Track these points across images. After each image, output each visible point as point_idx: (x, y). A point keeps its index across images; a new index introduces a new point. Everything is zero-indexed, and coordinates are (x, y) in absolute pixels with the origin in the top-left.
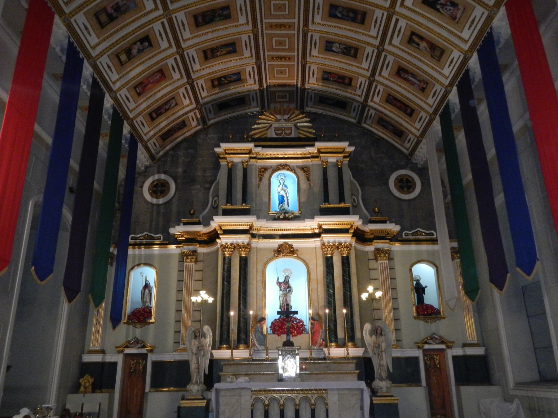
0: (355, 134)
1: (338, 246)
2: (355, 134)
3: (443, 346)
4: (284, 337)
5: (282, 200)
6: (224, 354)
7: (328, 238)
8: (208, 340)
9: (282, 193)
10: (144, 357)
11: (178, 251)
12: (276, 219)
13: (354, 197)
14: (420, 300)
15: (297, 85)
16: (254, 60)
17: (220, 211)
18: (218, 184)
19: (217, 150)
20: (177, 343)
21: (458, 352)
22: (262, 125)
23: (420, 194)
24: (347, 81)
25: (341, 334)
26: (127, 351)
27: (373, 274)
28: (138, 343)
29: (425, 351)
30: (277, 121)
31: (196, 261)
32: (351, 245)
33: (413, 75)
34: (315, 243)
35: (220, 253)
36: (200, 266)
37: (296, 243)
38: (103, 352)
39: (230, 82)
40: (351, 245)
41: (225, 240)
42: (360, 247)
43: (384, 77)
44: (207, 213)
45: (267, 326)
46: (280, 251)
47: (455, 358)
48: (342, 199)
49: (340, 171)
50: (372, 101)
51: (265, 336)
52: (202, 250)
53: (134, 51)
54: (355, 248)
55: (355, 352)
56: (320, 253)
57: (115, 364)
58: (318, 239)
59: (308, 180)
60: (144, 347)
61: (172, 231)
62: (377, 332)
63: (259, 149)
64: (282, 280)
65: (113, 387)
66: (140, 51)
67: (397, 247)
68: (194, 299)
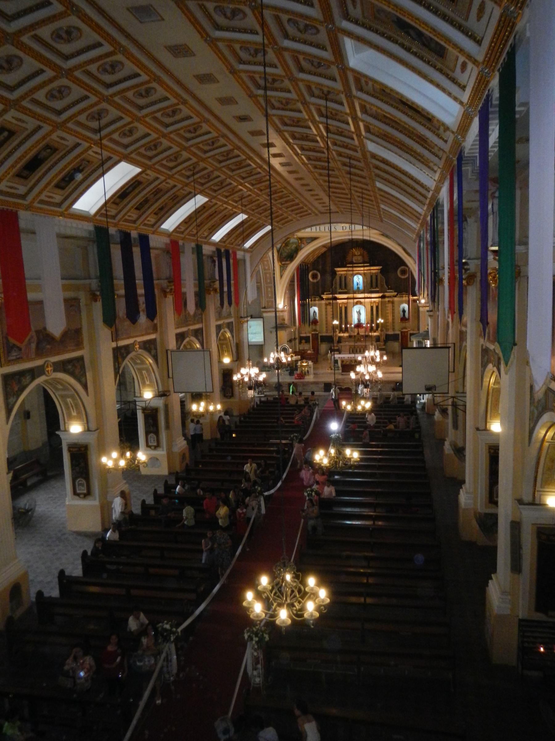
1: (374, 302)
3: (406, 330)
5: (358, 284)
6: (342, 335)
8: (338, 332)
10: (318, 334)
12: (354, 292)
19: (336, 269)
20: (327, 330)
28: (315, 330)
29: (402, 332)
37: (362, 300)
42: (384, 300)
46: (357, 303)
49: (377, 276)
61: (322, 296)
67: (396, 299)
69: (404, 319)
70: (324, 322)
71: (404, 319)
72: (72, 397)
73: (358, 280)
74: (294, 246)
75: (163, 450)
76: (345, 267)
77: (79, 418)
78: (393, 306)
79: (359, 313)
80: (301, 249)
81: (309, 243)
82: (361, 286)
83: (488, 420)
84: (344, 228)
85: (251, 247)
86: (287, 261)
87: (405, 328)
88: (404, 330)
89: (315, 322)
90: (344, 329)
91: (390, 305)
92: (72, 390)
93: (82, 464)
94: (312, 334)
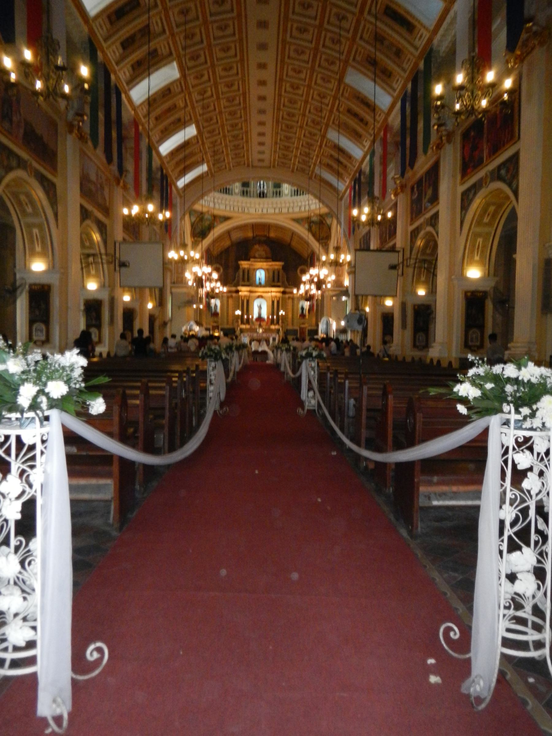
1: (276, 297)
4: (259, 323)
5: (259, 279)
6: (243, 326)
12: (257, 286)
18: (239, 274)
21: (310, 328)
25: (275, 322)
30: (258, 250)
45: (254, 319)
46: (259, 297)
48: (278, 281)
49: (279, 272)
52: (234, 295)
55: (277, 327)
59: (269, 273)
62: (283, 322)
64: (259, 305)
69: (303, 315)
70: (225, 314)
71: (303, 315)
72: (40, 227)
73: (261, 275)
75: (105, 346)
77: (44, 254)
78: (293, 302)
79: (260, 308)
80: (213, 228)
82: (263, 281)
83: (465, 266)
84: (257, 210)
85: (187, 186)
86: (199, 237)
87: (303, 324)
89: (215, 314)
90: (245, 321)
91: (290, 301)
92: (44, 217)
93: (43, 306)
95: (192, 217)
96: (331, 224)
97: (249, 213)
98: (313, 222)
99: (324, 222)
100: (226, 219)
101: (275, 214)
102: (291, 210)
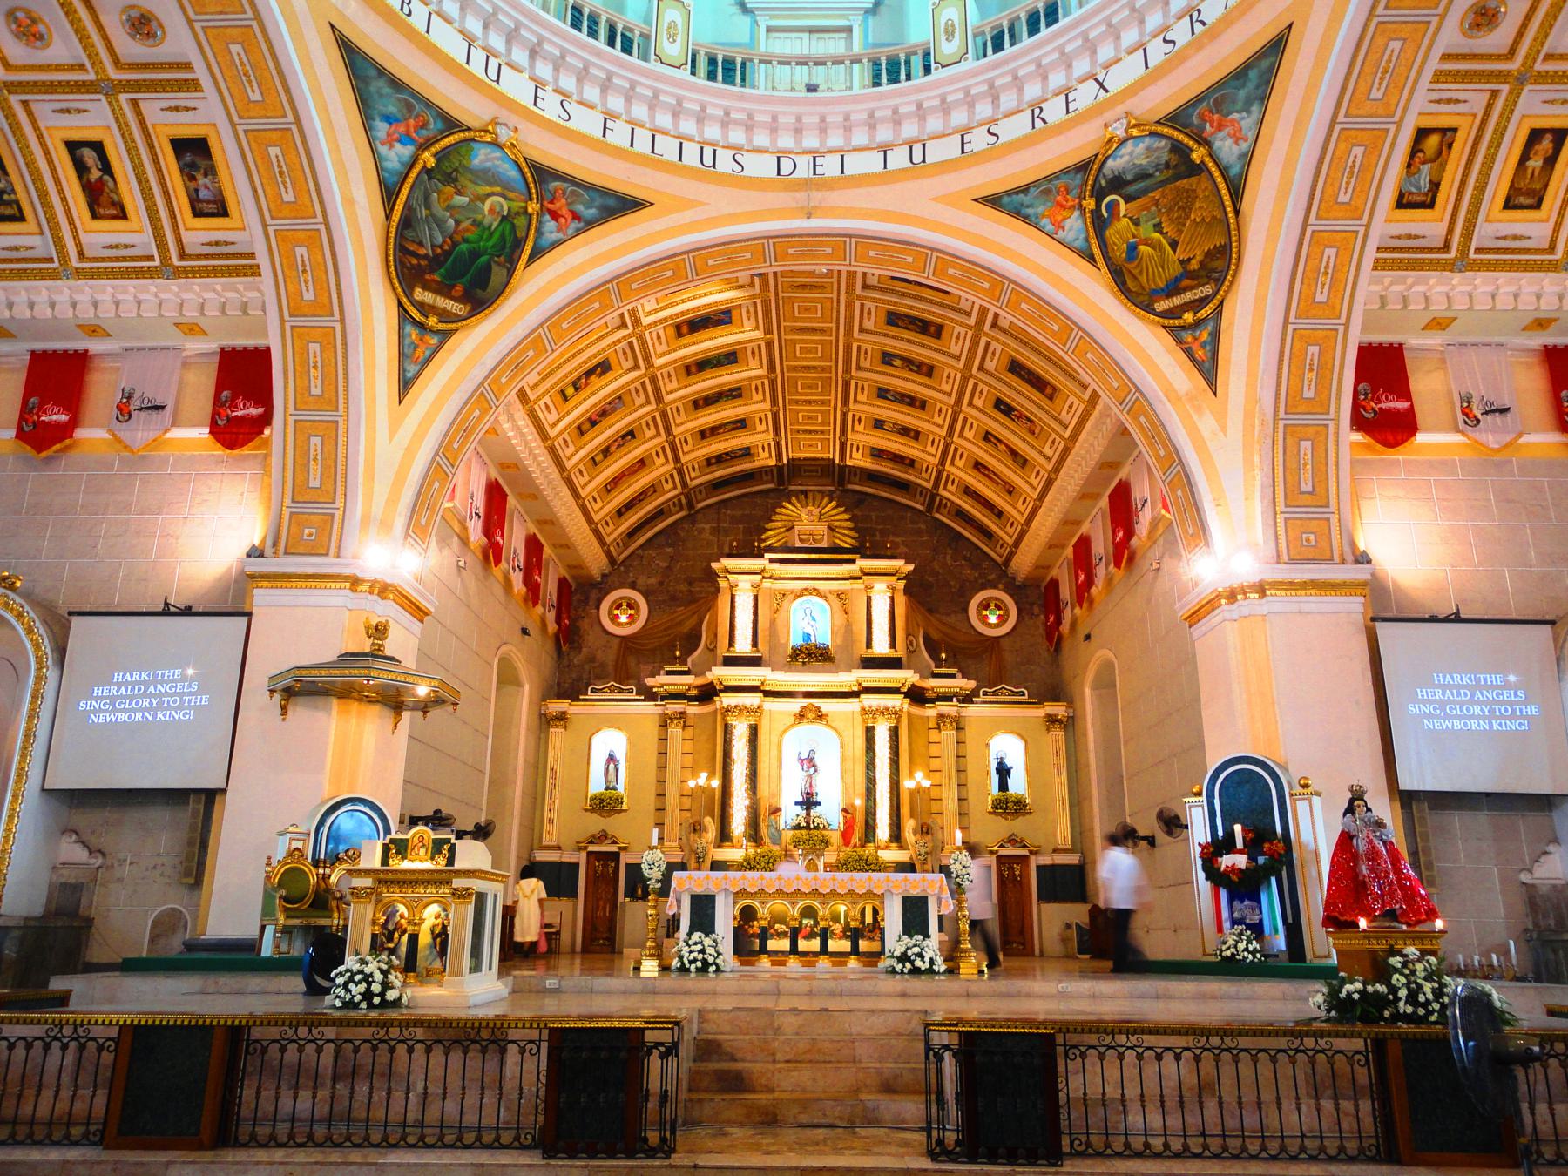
0: (923, 526)
1: (884, 712)
2: (923, 526)
3: (1024, 852)
7: (871, 701)
9: (809, 630)
10: (615, 857)
11: (659, 710)
13: (911, 638)
14: (1003, 786)
15: (834, 460)
16: (771, 436)
17: (720, 659)
19: (714, 565)
21: (1045, 860)
22: (779, 524)
23: (1014, 628)
24: (907, 462)
26: (592, 848)
27: (934, 750)
31: (684, 726)
32: (901, 711)
33: (995, 474)
34: (852, 705)
35: (719, 717)
36: (689, 733)
37: (826, 705)
38: (559, 848)
39: (732, 458)
40: (901, 711)
41: (727, 700)
43: (958, 468)
44: (699, 655)
46: (801, 716)
47: (1039, 868)
50: (945, 489)
51: (780, 832)
52: (693, 709)
53: (613, 449)
54: (909, 714)
56: (859, 719)
57: (577, 865)
58: (856, 700)
60: (615, 843)
62: (924, 830)
63: (776, 566)
64: (804, 756)
65: (574, 895)
66: (619, 446)
68: (692, 784)
74: (493, 205)
76: (762, 557)
80: (536, 254)
81: (590, 224)
86: (443, 290)
88: (1009, 851)
91: (949, 733)
94: (589, 854)
95: (382, 128)
96: (1247, 158)
97: (739, 181)
98: (1117, 183)
99: (1198, 155)
100: (621, 205)
101: (886, 177)
102: (979, 140)
